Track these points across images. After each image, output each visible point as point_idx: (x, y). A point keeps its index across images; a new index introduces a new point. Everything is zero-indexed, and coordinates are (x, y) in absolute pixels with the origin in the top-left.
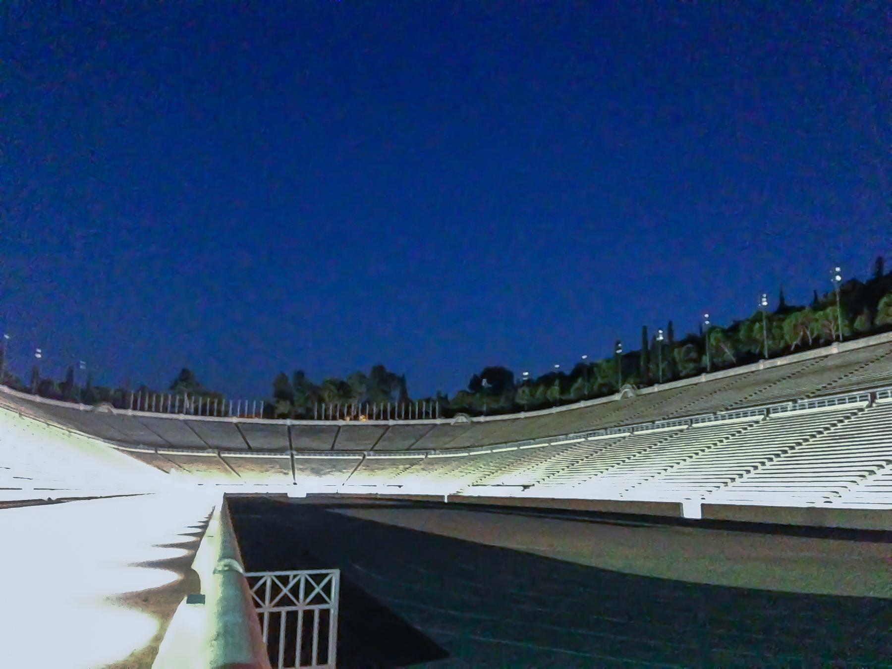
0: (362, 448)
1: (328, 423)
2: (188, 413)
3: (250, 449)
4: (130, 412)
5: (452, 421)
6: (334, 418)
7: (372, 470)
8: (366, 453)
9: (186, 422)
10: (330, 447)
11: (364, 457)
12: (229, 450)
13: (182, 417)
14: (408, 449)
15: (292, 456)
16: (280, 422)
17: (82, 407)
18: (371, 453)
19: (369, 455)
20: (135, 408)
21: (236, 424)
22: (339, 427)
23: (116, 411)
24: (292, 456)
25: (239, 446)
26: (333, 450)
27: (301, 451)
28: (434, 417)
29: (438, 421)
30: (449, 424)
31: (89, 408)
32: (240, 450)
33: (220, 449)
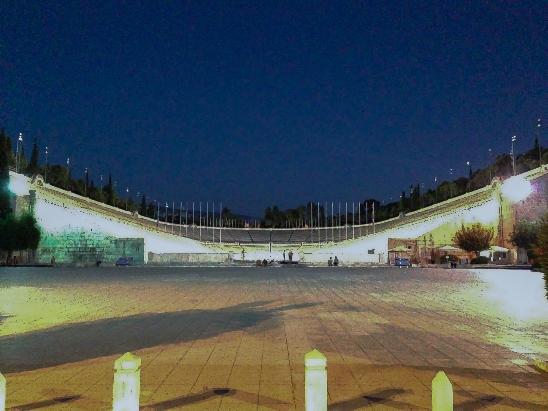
1: (288, 229)
2: (227, 227)
3: (253, 242)
6: (291, 227)
8: (303, 243)
9: (226, 230)
10: (287, 241)
11: (302, 244)
12: (245, 242)
15: (271, 244)
18: (305, 243)
19: (304, 244)
22: (293, 231)
24: (271, 244)
26: (289, 242)
27: (275, 242)
32: (249, 242)
33: (240, 242)
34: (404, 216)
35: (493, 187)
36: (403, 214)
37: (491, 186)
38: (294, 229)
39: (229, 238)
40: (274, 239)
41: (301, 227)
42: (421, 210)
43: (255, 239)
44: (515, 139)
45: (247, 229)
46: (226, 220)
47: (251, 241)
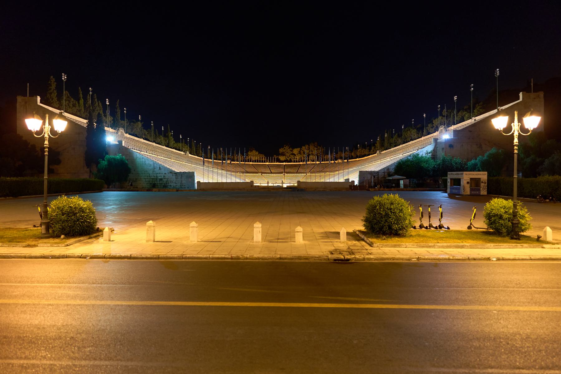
0: (307, 171)
1: (297, 163)
2: (253, 162)
3: (271, 173)
6: (299, 162)
9: (252, 164)
13: (251, 163)
14: (321, 171)
15: (284, 174)
18: (309, 173)
20: (237, 161)
22: (301, 164)
24: (284, 174)
25: (268, 172)
26: (297, 172)
27: (287, 173)
32: (268, 173)
33: (262, 173)
34: (380, 154)
35: (440, 133)
36: (380, 152)
37: (438, 132)
38: (301, 163)
39: (254, 170)
40: (287, 170)
42: (392, 149)
44: (456, 98)
45: (267, 163)
46: (252, 157)
47: (270, 172)
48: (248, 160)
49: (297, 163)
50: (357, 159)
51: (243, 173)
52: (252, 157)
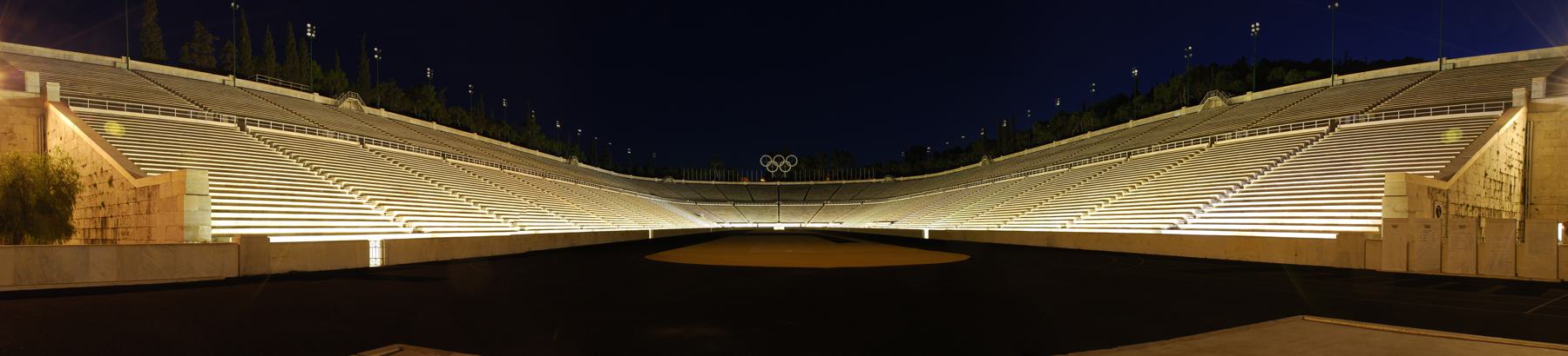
1: (804, 183)
2: (717, 180)
3: (753, 201)
4: (683, 181)
5: (882, 180)
6: (808, 180)
7: (827, 213)
9: (716, 185)
12: (743, 202)
13: (713, 182)
16: (774, 183)
17: (656, 180)
21: (746, 186)
23: (675, 181)
26: (805, 201)
27: (785, 201)
28: (872, 178)
29: (874, 180)
30: (880, 182)
31: (660, 180)
32: (747, 202)
38: (812, 183)
39: (720, 196)
41: (821, 180)
43: (755, 198)
45: (745, 183)
46: (715, 171)
47: (750, 199)
48: (708, 176)
49: (804, 183)
50: (926, 176)
51: (696, 201)
52: (715, 171)
